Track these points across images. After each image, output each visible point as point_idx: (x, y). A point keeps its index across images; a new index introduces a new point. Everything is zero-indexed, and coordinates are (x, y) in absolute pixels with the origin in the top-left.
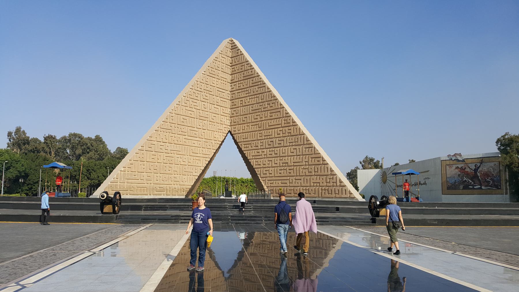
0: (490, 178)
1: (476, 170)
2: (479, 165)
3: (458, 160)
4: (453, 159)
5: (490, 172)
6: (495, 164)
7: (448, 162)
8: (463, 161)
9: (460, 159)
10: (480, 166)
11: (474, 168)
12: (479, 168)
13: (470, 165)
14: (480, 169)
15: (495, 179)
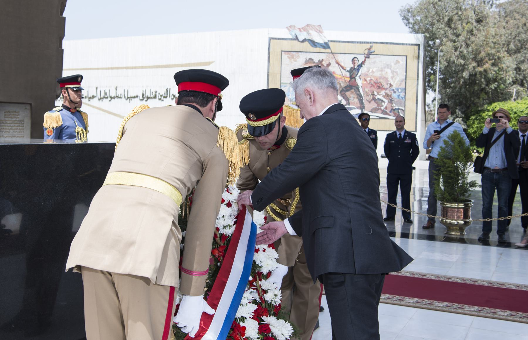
0: (383, 92)
1: (353, 72)
2: (361, 58)
3: (313, 43)
4: (301, 38)
5: (387, 80)
6: (398, 62)
7: (287, 46)
8: (326, 46)
9: (318, 39)
10: (363, 63)
11: (349, 65)
12: (360, 66)
13: (340, 58)
14: (363, 70)
15: (395, 96)
